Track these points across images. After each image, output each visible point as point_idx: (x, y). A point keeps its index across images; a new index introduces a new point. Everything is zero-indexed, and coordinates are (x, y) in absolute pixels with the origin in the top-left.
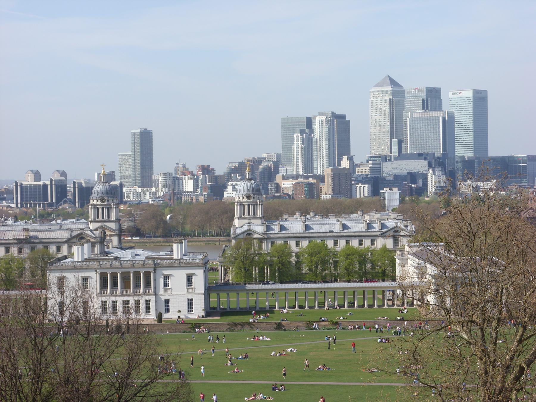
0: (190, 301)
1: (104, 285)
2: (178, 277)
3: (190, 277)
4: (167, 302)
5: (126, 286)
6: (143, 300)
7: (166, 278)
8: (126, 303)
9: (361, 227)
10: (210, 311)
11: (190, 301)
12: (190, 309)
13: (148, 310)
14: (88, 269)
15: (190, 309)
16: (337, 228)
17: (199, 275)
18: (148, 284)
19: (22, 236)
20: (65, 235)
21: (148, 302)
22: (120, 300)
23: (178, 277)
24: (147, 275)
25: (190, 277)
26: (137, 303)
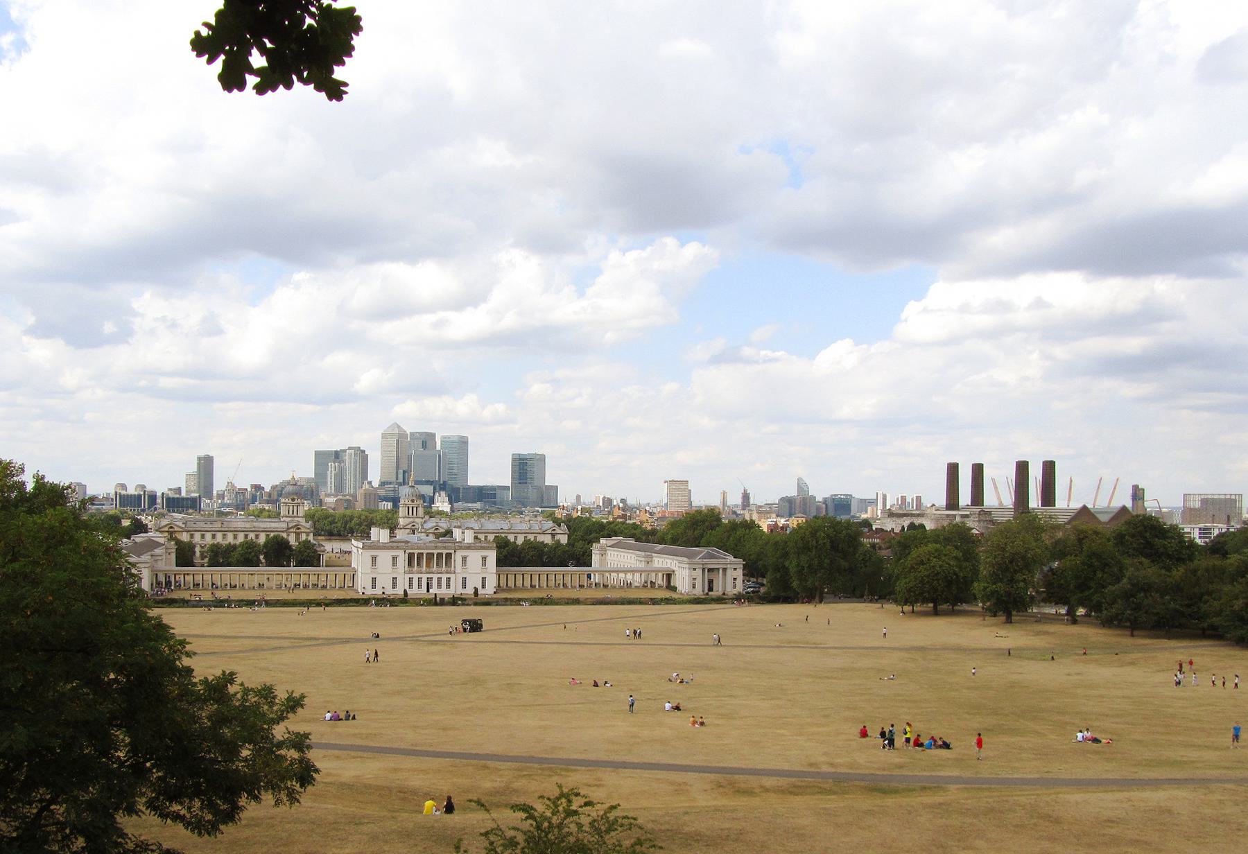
0: (484, 579)
1: (410, 563)
3: (484, 558)
4: (464, 579)
5: (428, 565)
6: (444, 577)
7: (464, 559)
8: (430, 579)
10: (499, 589)
11: (484, 579)
12: (484, 586)
13: (448, 586)
14: (398, 548)
15: (484, 586)
16: (506, 527)
17: (492, 556)
18: (448, 563)
19: (248, 525)
20: (284, 526)
21: (448, 579)
22: (425, 577)
23: (474, 557)
24: (449, 556)
25: (484, 558)
26: (430, 579)
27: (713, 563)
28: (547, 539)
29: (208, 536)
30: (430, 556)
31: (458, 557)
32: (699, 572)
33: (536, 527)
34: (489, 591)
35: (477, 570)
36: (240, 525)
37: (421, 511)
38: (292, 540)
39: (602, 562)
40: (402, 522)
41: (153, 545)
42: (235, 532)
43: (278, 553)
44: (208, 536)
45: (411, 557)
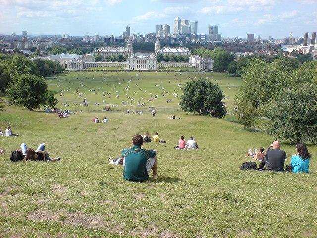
1: (137, 62)
2: (151, 61)
9: (181, 51)
16: (176, 51)
17: (155, 61)
27: (206, 62)
28: (185, 54)
29: (107, 54)
30: (141, 61)
31: (148, 61)
32: (202, 65)
33: (184, 51)
34: (155, 69)
35: (152, 64)
36: (114, 51)
37: (160, 46)
38: (124, 55)
39: (191, 62)
40: (155, 49)
41: (89, 56)
42: (113, 52)
43: (121, 58)
44: (107, 54)
45: (137, 61)
